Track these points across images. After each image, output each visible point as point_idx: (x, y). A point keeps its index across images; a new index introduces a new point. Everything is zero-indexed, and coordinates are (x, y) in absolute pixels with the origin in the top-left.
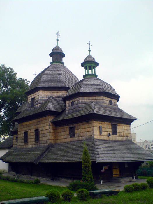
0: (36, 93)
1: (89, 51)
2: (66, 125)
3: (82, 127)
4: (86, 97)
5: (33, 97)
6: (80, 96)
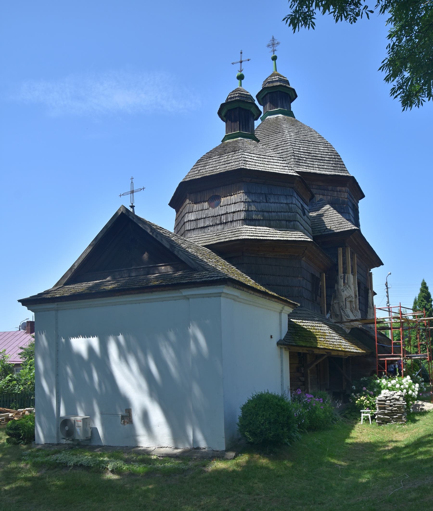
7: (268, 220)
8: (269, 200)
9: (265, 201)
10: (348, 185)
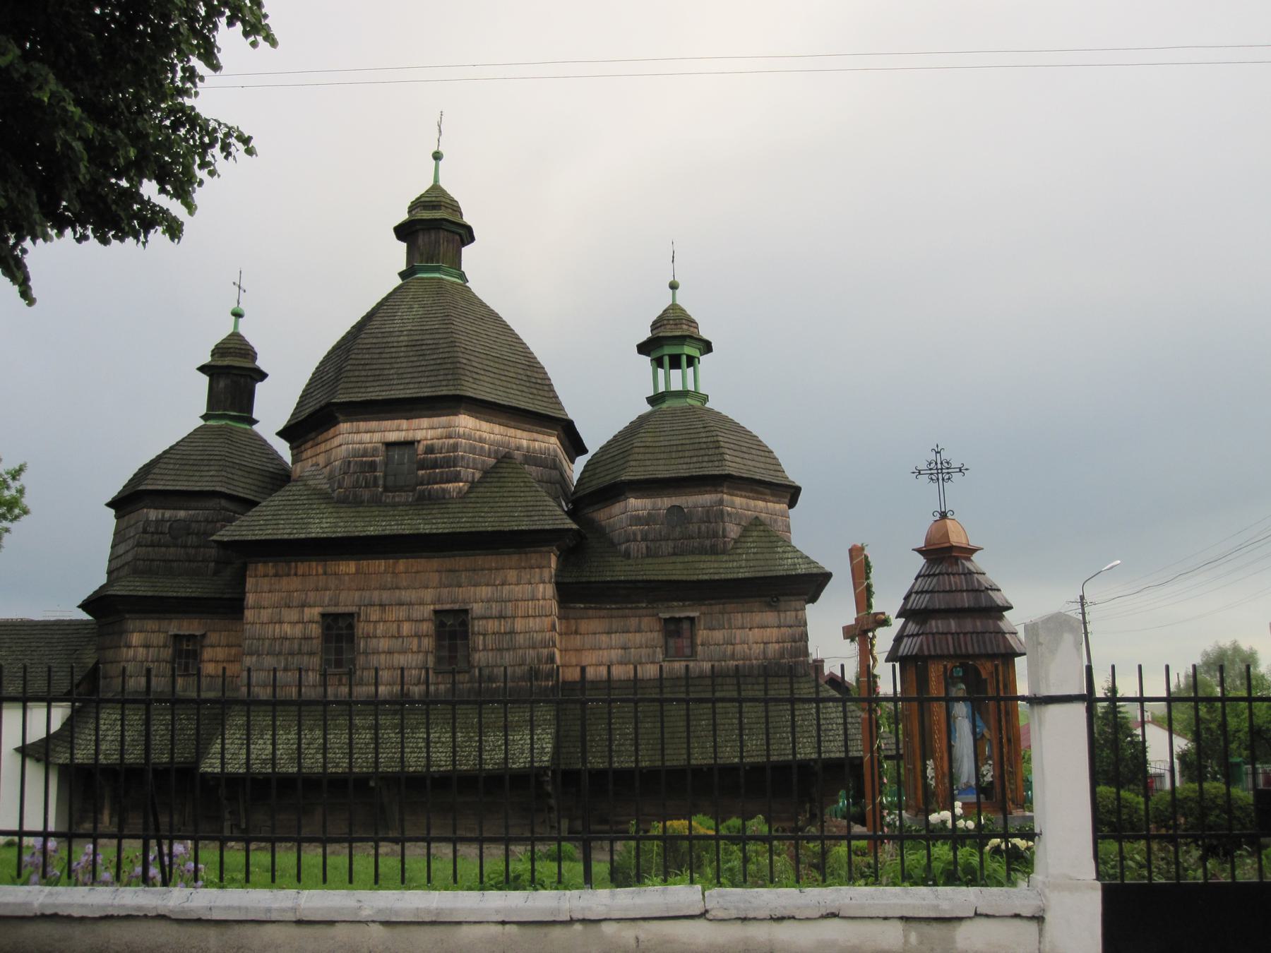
0: (425, 422)
1: (673, 286)
2: (644, 605)
3: (738, 619)
4: (741, 496)
5: (393, 437)
6: (725, 491)
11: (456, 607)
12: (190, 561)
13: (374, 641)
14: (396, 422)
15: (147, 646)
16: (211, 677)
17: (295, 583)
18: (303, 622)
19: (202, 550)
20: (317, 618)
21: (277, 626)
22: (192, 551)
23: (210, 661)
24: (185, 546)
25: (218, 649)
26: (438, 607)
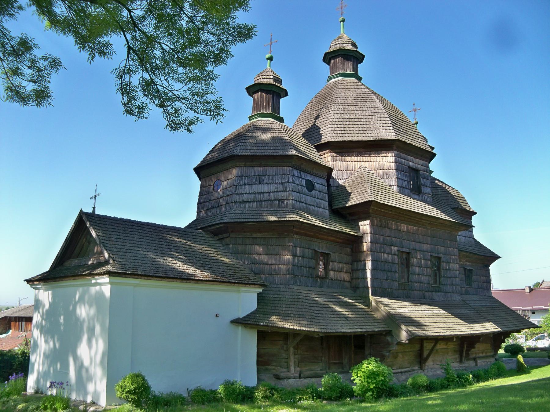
0: (420, 161)
5: (411, 164)
7: (259, 201)
8: (262, 182)
9: (258, 183)
10: (395, 148)
11: (436, 255)
12: (318, 207)
13: (414, 268)
14: (412, 158)
15: (303, 257)
16: (332, 279)
17: (387, 232)
18: (391, 254)
19: (322, 201)
20: (397, 253)
21: (383, 254)
22: (317, 200)
23: (332, 270)
24: (315, 198)
25: (335, 264)
26: (431, 254)
